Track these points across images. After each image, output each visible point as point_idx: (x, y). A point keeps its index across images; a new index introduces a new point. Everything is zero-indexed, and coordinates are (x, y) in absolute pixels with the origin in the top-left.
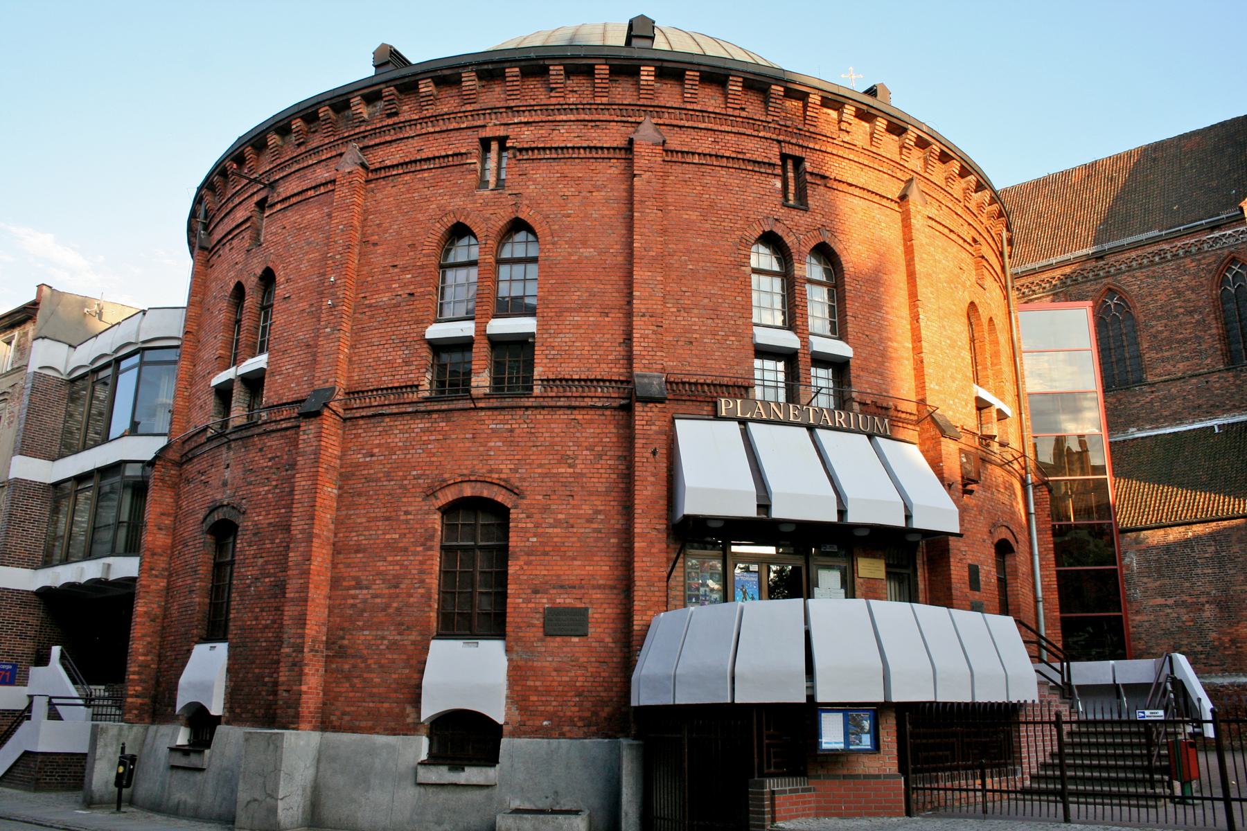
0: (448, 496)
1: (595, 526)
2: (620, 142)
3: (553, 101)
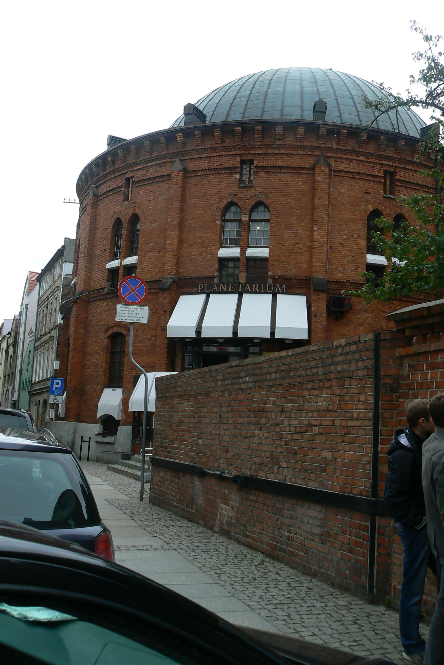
0: (110, 332)
1: (151, 342)
2: (169, 172)
3: (148, 157)
